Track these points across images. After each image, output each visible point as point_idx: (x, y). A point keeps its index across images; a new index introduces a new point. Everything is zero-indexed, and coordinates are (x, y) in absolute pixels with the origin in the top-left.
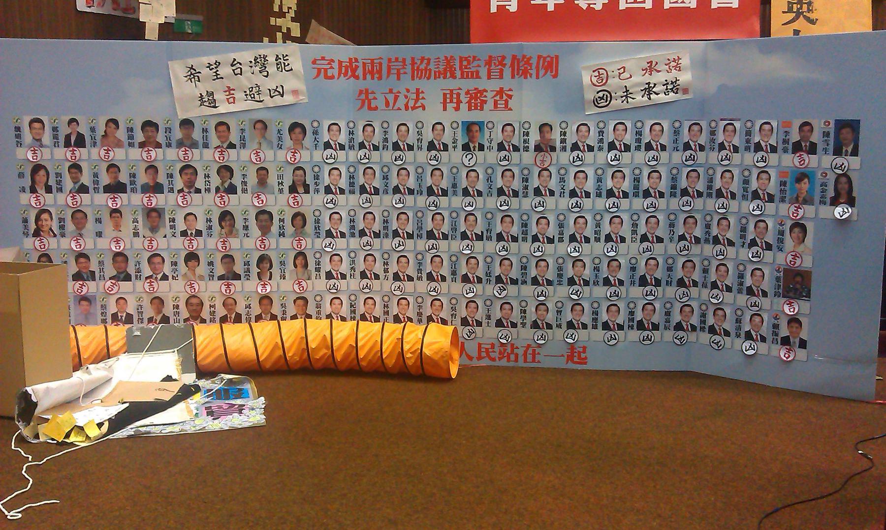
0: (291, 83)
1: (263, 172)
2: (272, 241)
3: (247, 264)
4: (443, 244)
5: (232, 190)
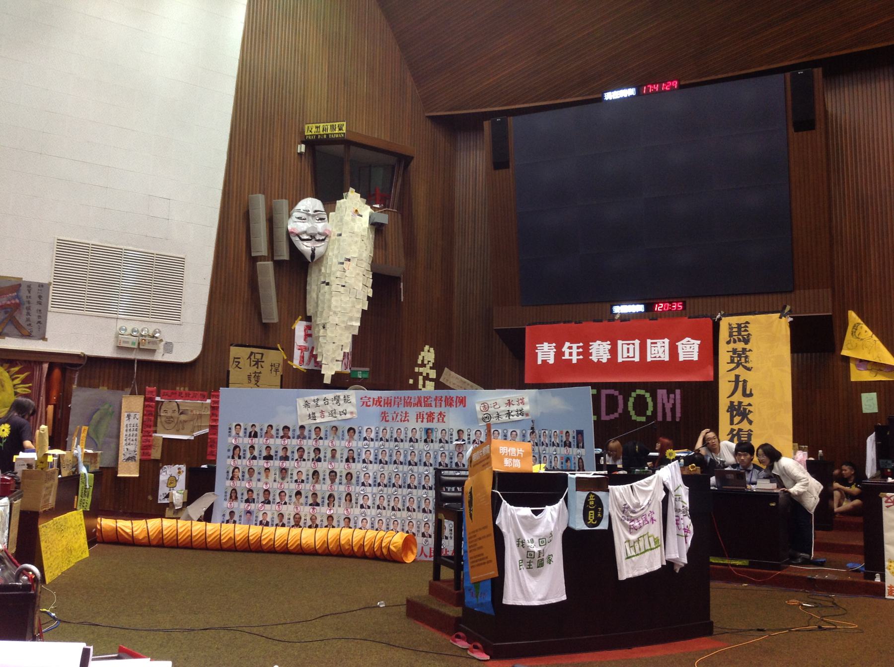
0: (350, 408)
1: (334, 451)
2: (335, 487)
3: (323, 498)
4: (414, 491)
5: (319, 460)
